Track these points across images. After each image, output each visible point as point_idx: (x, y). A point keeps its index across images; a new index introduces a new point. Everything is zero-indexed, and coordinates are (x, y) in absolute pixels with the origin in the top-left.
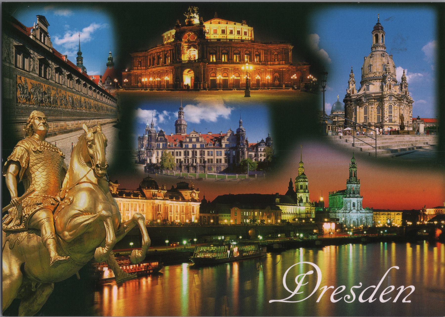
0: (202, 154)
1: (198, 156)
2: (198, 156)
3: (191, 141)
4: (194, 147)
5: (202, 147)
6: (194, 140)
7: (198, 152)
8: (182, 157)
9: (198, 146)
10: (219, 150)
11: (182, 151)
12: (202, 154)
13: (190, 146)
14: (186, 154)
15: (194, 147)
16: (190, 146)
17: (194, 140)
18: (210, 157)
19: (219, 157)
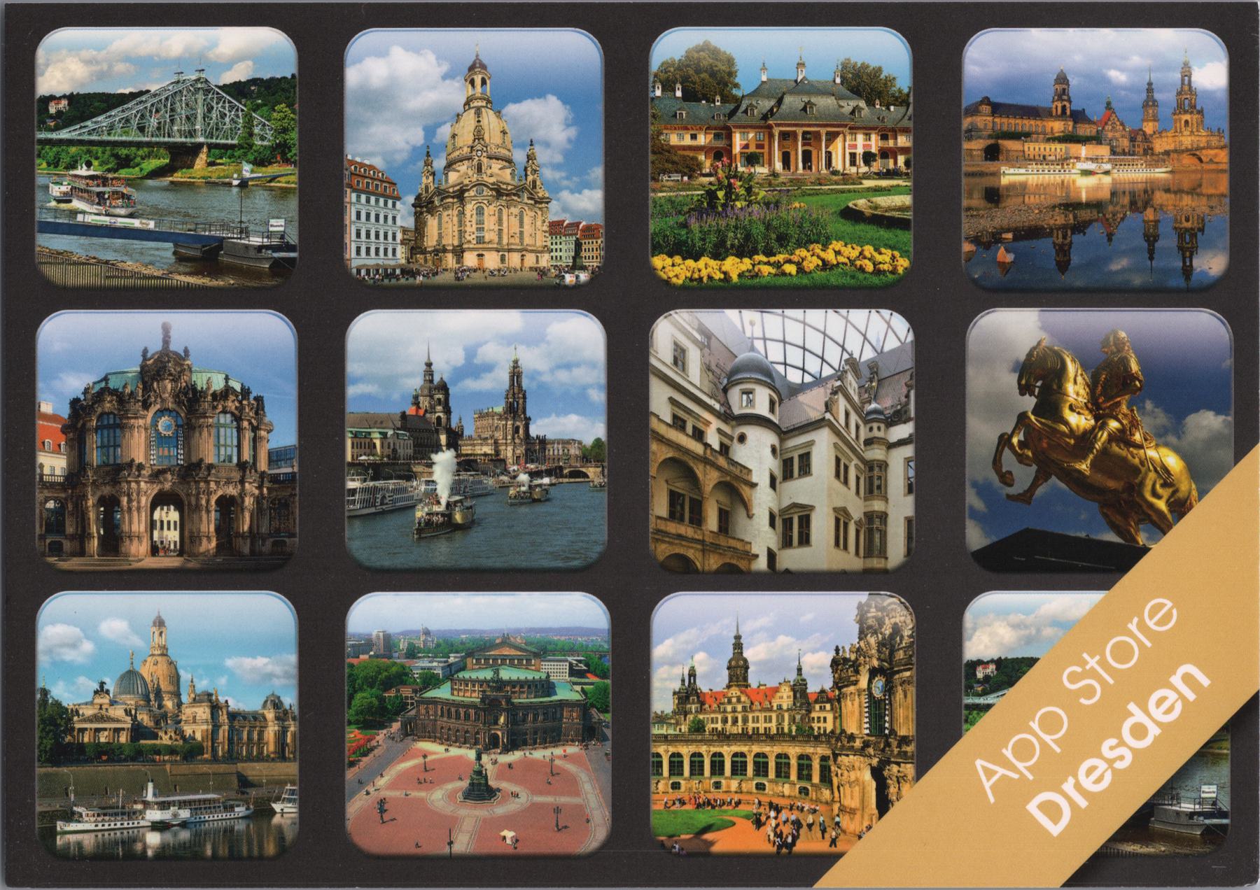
0: (745, 720)
1: (740, 723)
2: (740, 723)
3: (730, 702)
4: (734, 711)
5: (744, 709)
6: (734, 700)
7: (740, 717)
8: (719, 726)
9: (739, 708)
10: (768, 714)
11: (720, 717)
12: (745, 720)
13: (729, 708)
14: (725, 721)
15: (734, 711)
16: (729, 708)
17: (734, 700)
18: (756, 725)
19: (768, 725)
